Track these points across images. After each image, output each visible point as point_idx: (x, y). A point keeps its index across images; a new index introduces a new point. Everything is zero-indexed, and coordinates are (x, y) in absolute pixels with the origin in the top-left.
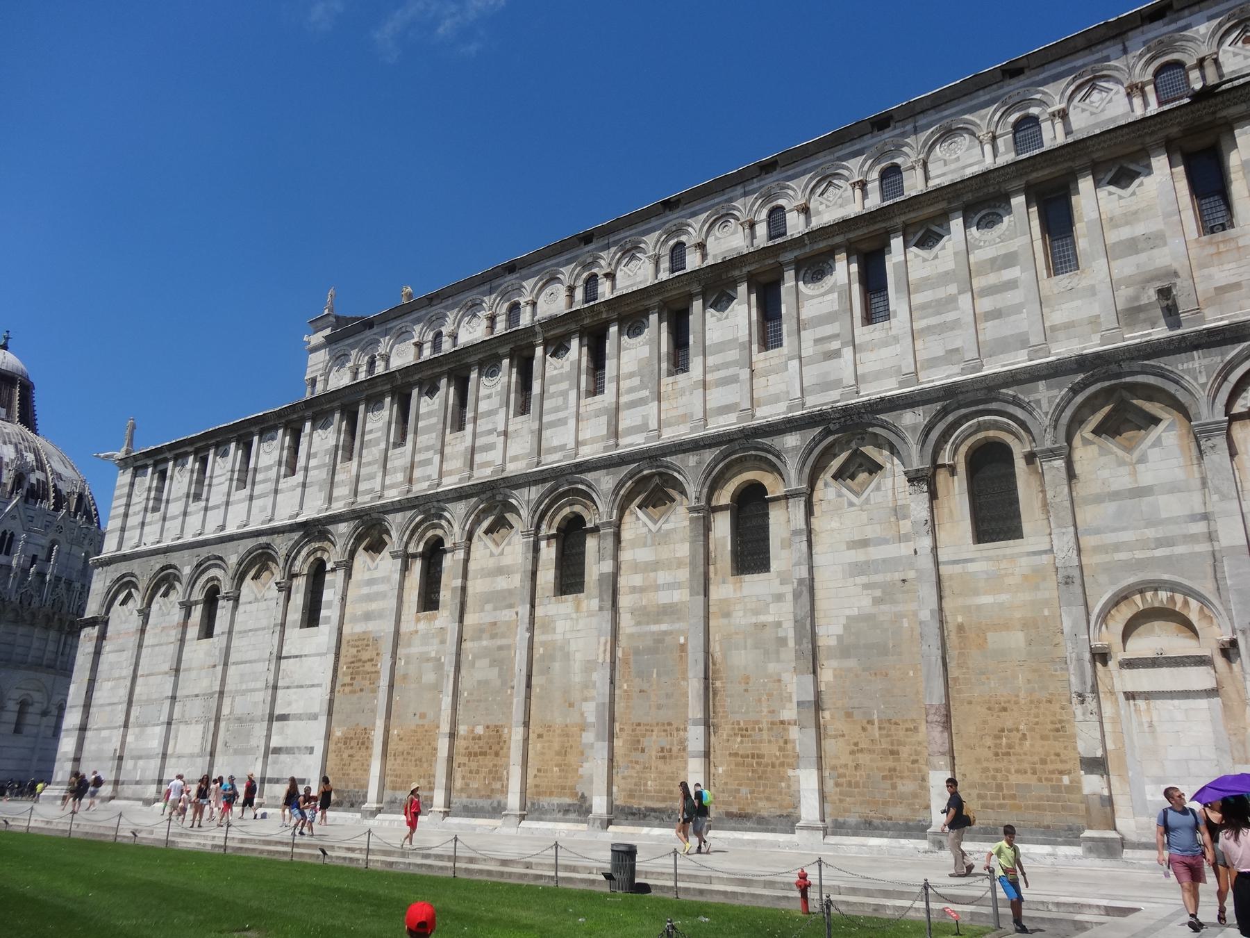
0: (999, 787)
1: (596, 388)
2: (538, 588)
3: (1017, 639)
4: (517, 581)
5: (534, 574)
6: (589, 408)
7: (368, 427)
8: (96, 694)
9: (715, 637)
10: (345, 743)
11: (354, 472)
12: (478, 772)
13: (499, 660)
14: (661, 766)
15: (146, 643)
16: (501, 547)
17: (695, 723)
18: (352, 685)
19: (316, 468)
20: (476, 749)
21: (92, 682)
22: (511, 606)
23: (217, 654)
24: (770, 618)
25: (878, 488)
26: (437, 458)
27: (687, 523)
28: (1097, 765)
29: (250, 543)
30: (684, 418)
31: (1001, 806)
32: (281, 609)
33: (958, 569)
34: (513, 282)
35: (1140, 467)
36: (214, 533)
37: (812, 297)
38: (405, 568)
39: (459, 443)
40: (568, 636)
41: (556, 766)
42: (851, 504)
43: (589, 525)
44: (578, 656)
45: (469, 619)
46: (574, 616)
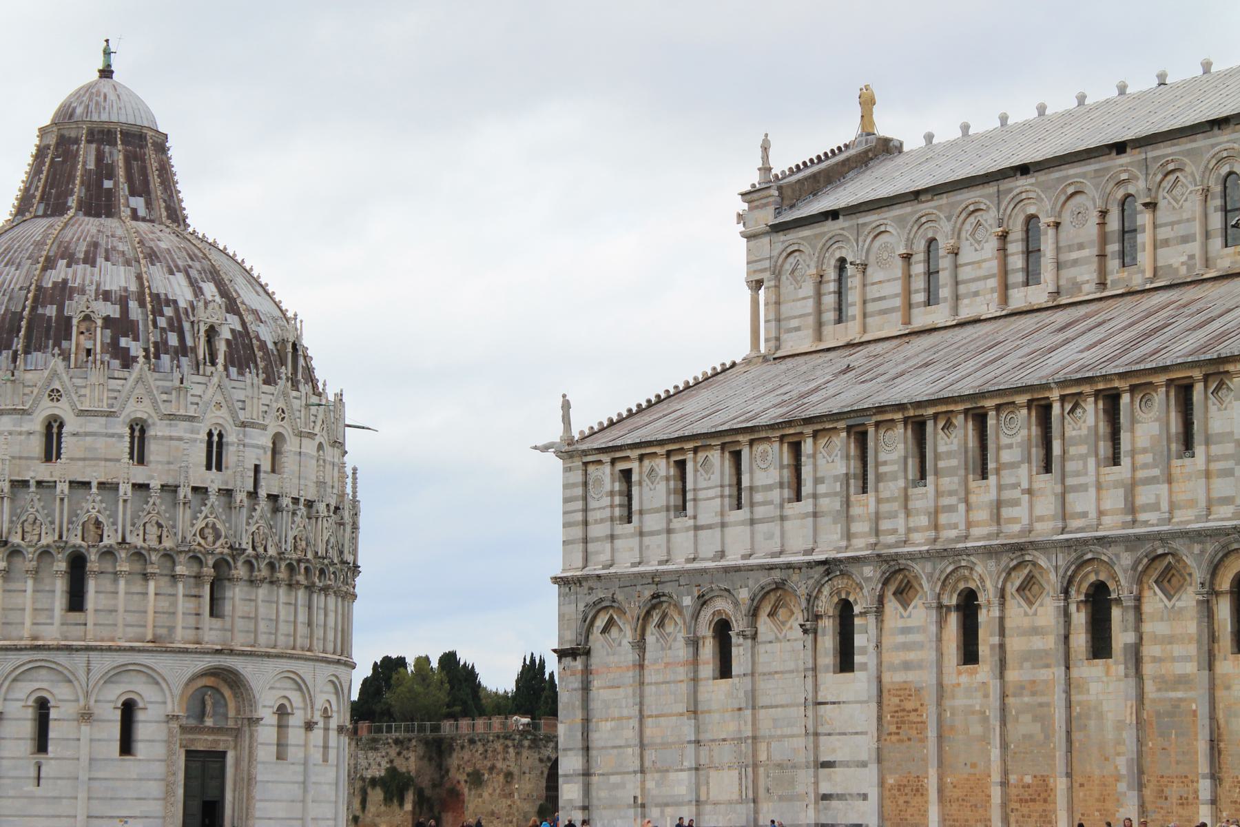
1: (1115, 460)
2: (1072, 650)
4: (1050, 642)
5: (1067, 637)
6: (1108, 478)
7: (883, 457)
8: (594, 736)
9: (1221, 706)
10: (899, 790)
11: (872, 508)
12: (1029, 816)
13: (1041, 715)
14: (1181, 811)
16: (1034, 607)
17: (1204, 777)
18: (898, 734)
19: (826, 495)
21: (586, 721)
22: (1048, 666)
23: (742, 694)
26: (962, 507)
27: (1194, 603)
29: (765, 579)
30: (1192, 503)
32: (810, 652)
34: (1028, 188)
36: (713, 560)
38: (941, 623)
39: (985, 493)
40: (1101, 697)
41: (1097, 811)
44: (1110, 715)
45: (1012, 675)
46: (1105, 679)
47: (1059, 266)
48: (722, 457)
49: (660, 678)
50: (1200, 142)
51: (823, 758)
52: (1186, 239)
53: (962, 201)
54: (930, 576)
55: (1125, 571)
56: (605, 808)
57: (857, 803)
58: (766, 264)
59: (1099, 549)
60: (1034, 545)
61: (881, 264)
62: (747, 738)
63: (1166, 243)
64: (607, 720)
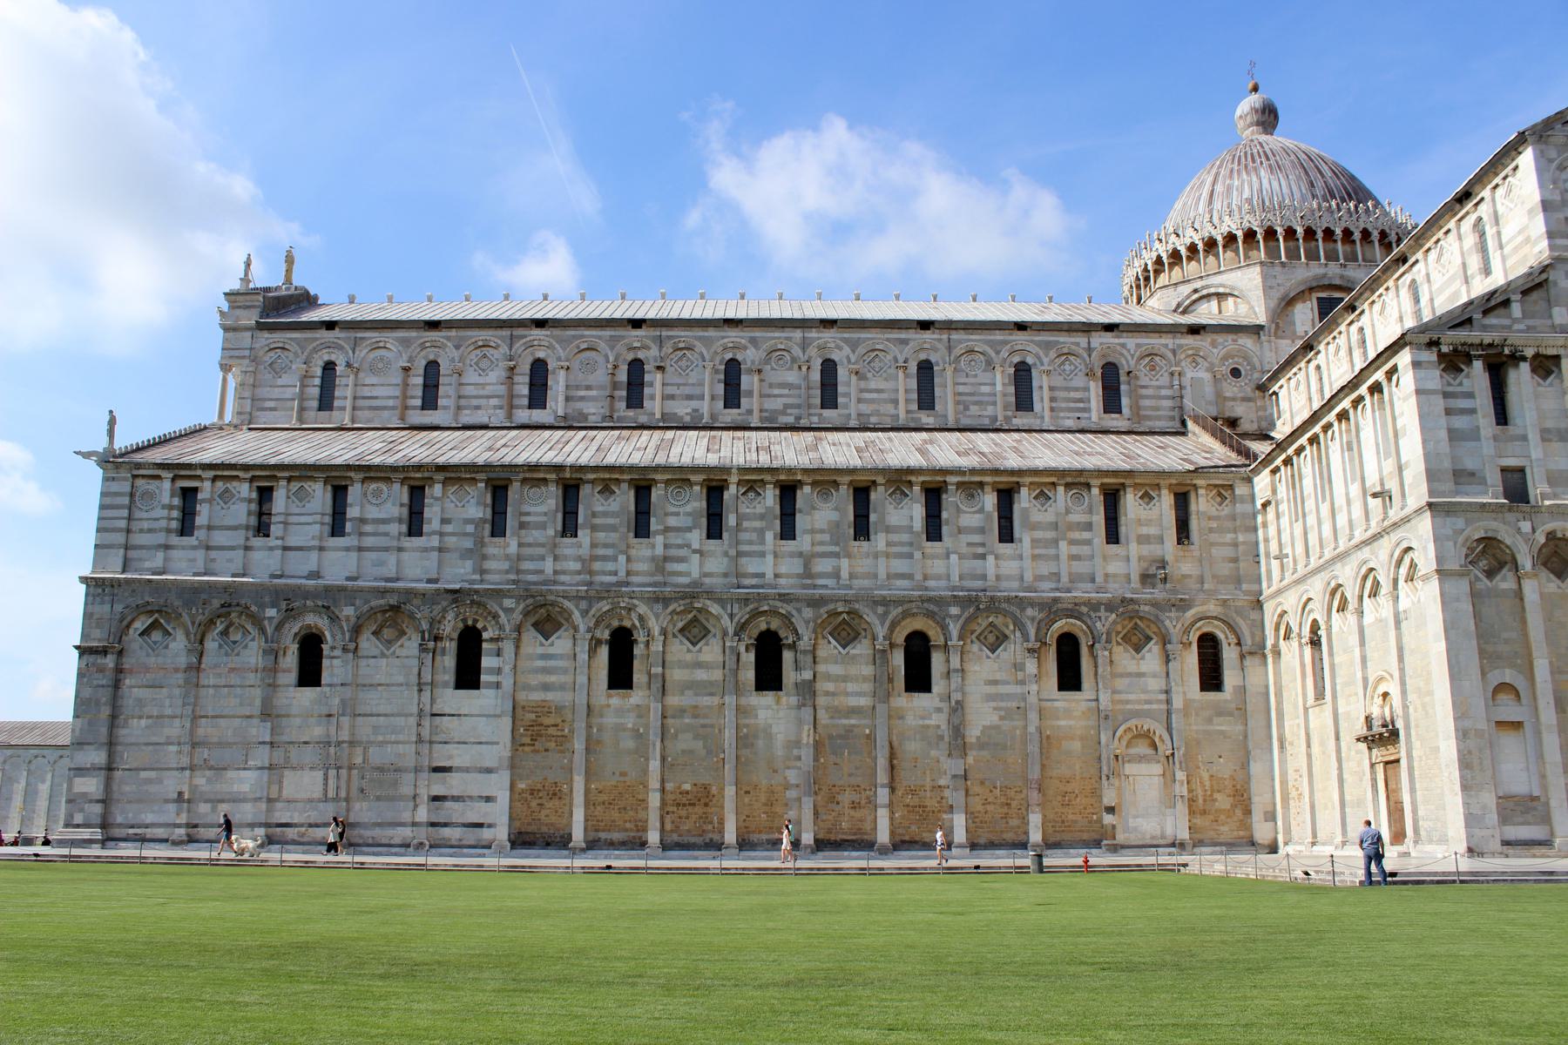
0: (1063, 822)
3: (1076, 746)
4: (717, 675)
12: (687, 818)
14: (852, 813)
15: (204, 681)
17: (883, 786)
20: (684, 800)
22: (712, 694)
24: (932, 722)
25: (1005, 650)
26: (622, 559)
28: (1111, 810)
33: (1049, 704)
36: (307, 578)
38: (592, 652)
40: (770, 721)
42: (988, 657)
43: (785, 642)
45: (673, 700)
47: (568, 399)
48: (325, 489)
49: (222, 681)
50: (711, 333)
51: (435, 764)
52: (690, 397)
53: (471, 337)
54: (585, 613)
55: (807, 622)
56: (130, 802)
57: (477, 804)
58: (247, 353)
59: (778, 604)
60: (710, 594)
61: (373, 370)
62: (343, 742)
63: (672, 397)
64: (140, 717)
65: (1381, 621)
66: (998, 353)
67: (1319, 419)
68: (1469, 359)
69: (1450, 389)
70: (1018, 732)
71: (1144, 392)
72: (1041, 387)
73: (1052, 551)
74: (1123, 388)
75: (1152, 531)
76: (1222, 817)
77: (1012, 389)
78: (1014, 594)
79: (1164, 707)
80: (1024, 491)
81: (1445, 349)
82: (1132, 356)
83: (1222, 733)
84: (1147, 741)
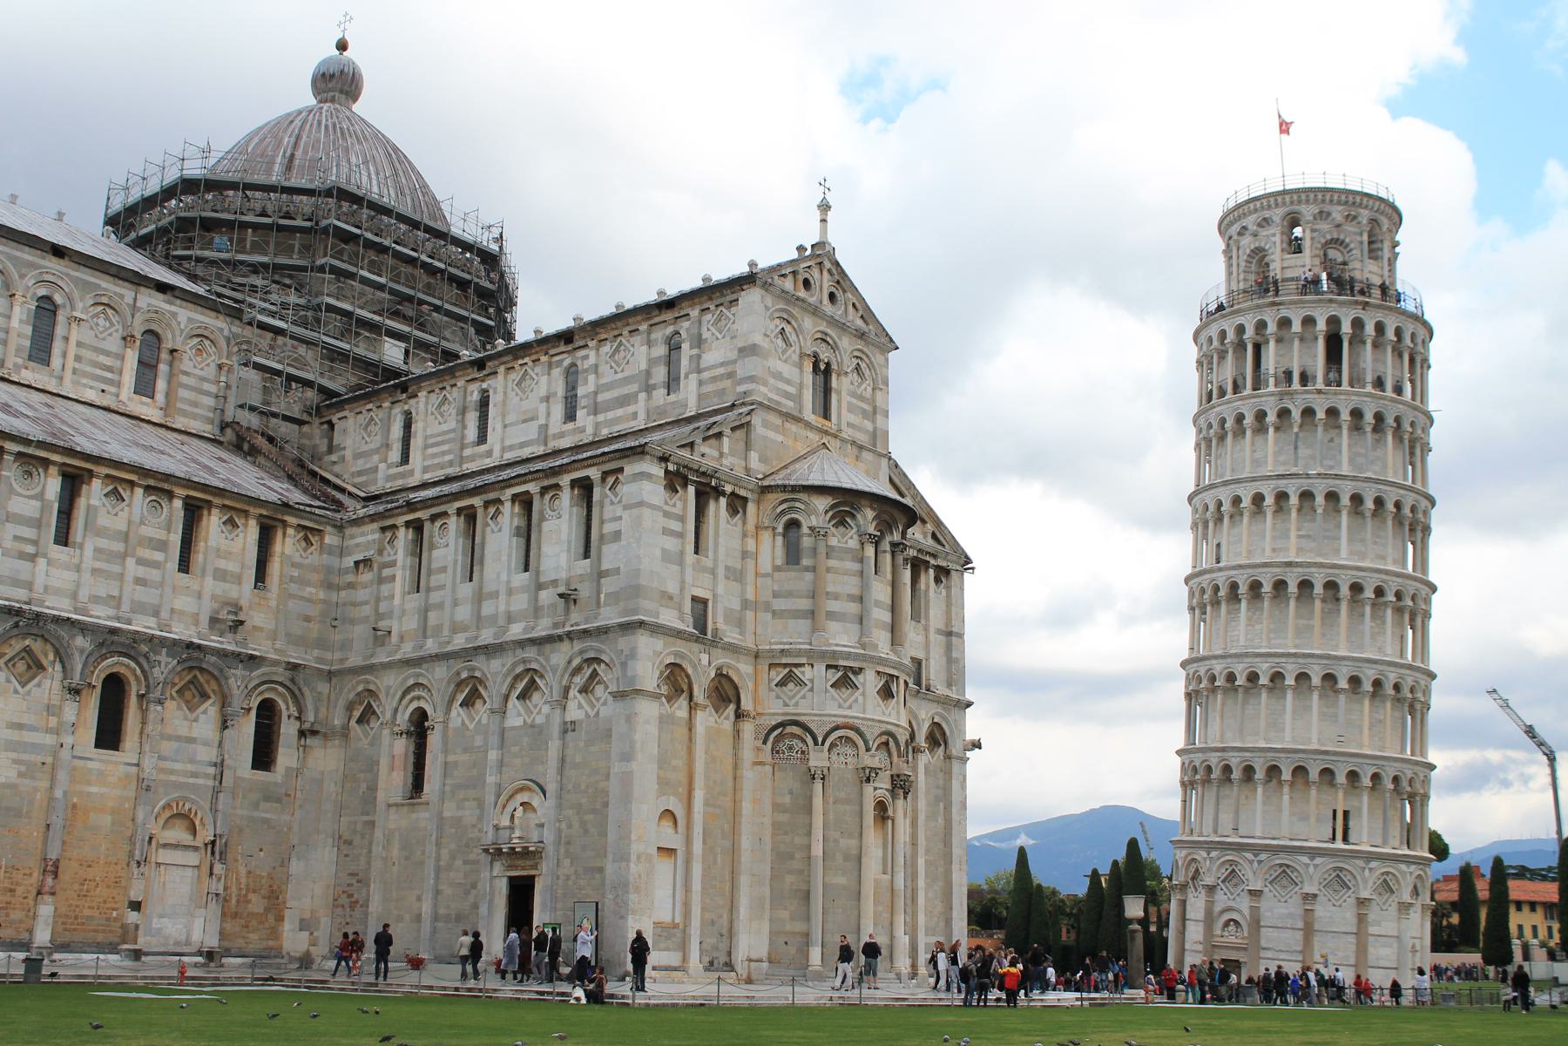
0: (76, 918)
3: (107, 820)
25: (39, 685)
28: (136, 906)
31: (74, 930)
35: (194, 724)
37: (20, 495)
42: (16, 692)
65: (532, 726)
66: (22, 276)
67: (485, 492)
68: (685, 482)
69: (667, 508)
70: (39, 796)
71: (184, 379)
72: (66, 339)
73: (116, 569)
74: (163, 368)
75: (232, 567)
76: (254, 923)
77: (29, 330)
78: (66, 615)
79: (210, 783)
80: (96, 484)
81: (671, 467)
82: (182, 331)
83: (266, 821)
84: (186, 822)
